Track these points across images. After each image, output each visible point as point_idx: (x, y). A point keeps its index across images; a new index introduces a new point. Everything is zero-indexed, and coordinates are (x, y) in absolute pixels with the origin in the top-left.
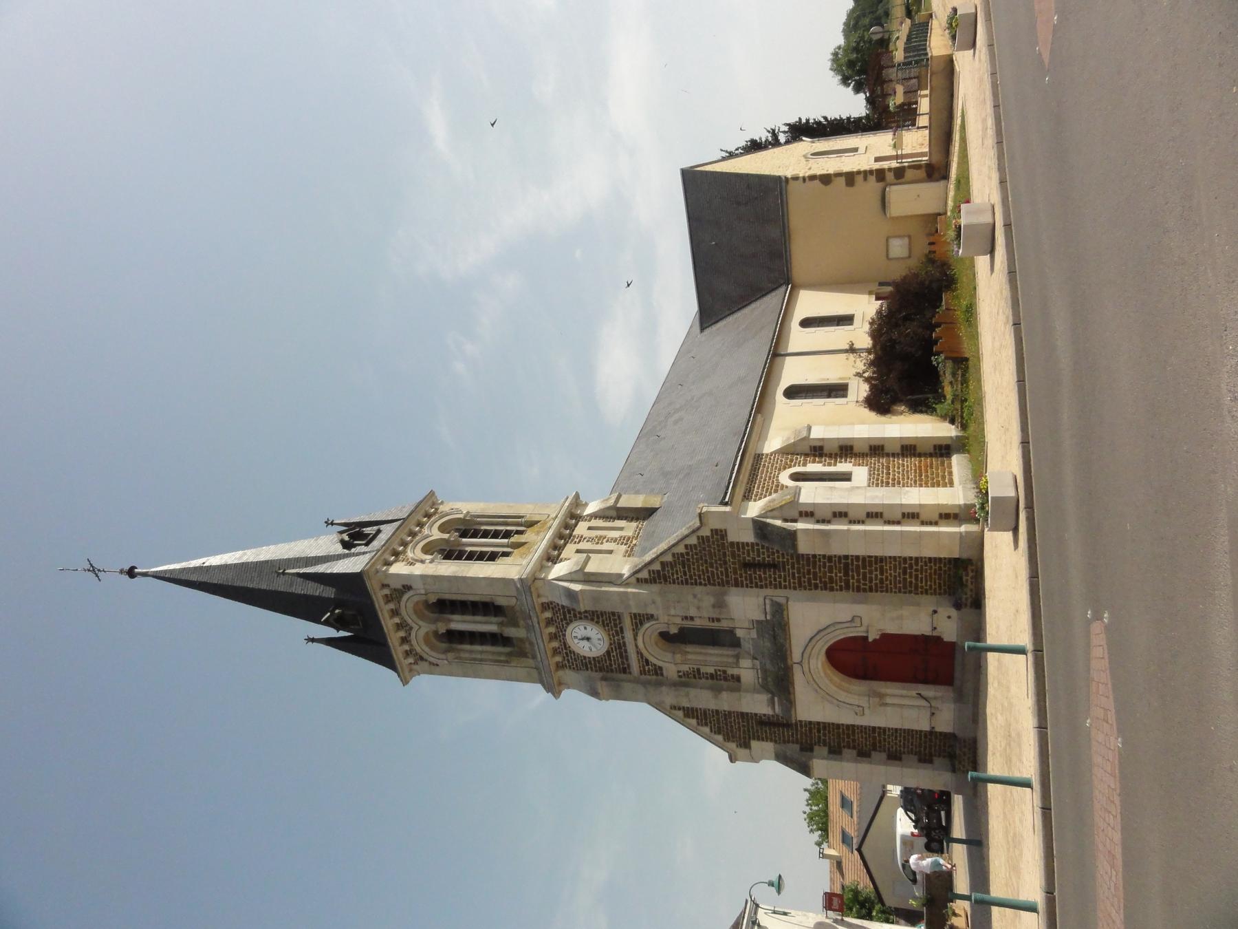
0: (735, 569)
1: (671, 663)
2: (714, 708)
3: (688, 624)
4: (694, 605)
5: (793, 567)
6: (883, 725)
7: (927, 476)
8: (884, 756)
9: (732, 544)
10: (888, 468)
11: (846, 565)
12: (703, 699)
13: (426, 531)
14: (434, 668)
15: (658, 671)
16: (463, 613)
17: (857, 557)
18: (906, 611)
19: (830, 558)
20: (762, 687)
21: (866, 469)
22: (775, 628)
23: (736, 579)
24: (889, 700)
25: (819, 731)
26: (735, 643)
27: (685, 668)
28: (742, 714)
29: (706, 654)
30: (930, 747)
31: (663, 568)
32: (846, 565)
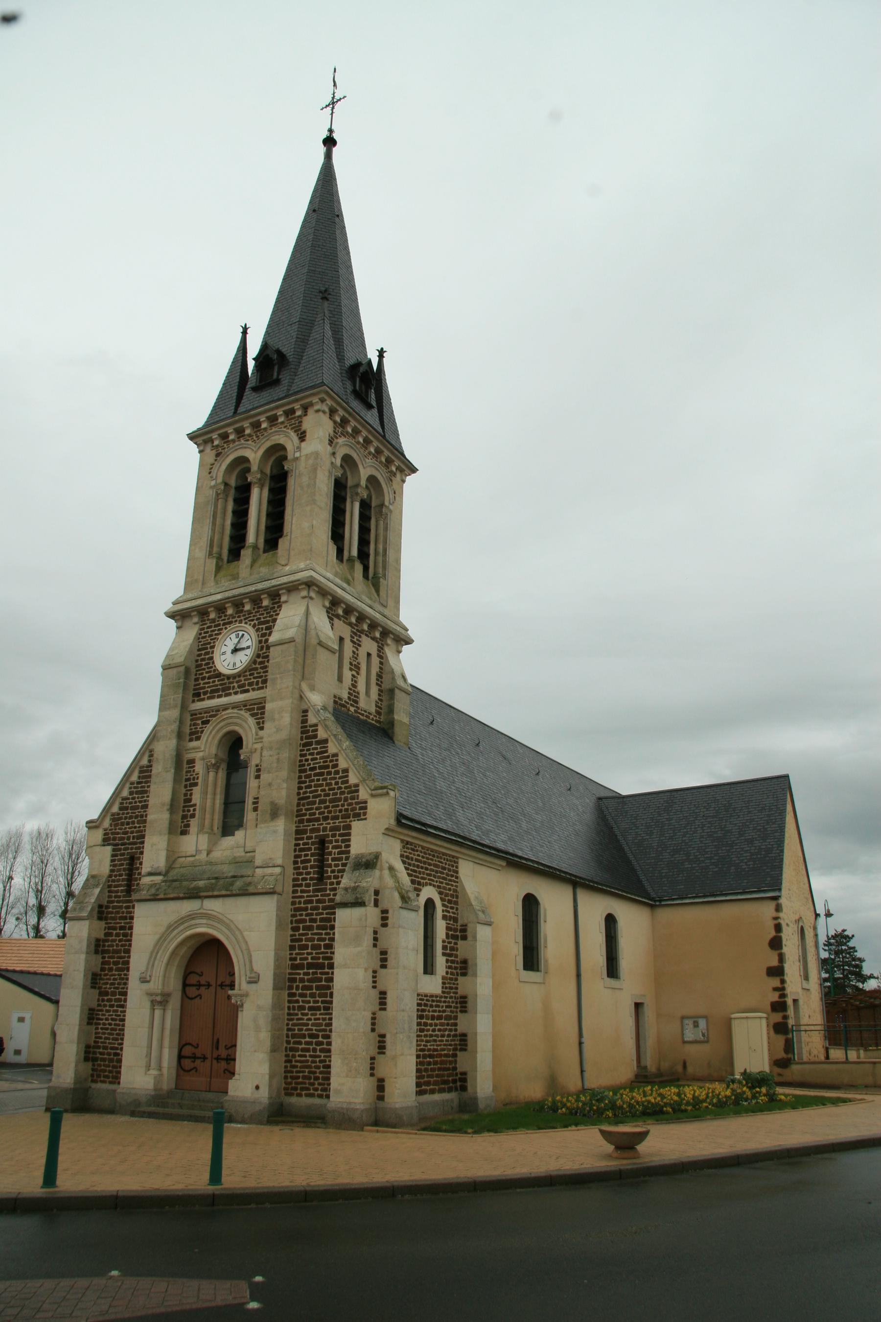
0: (318, 830)
1: (206, 748)
2: (151, 803)
3: (251, 771)
4: (273, 781)
5: (318, 901)
6: (129, 1004)
7: (429, 1063)
8: (94, 1004)
9: (349, 827)
10: (439, 1018)
11: (322, 966)
12: (161, 792)
13: (369, 461)
14: (206, 470)
15: (195, 735)
16: (270, 502)
17: (331, 980)
18: (265, 1036)
19: (330, 946)
20: (242, 826)
21: (438, 991)
22: (235, 885)
23: (305, 832)
24: (158, 1013)
25: (121, 928)
26: (227, 830)
27: (199, 768)
28: (143, 837)
29: (215, 794)
30: (104, 1060)
31: (318, 743)
32: (322, 966)
